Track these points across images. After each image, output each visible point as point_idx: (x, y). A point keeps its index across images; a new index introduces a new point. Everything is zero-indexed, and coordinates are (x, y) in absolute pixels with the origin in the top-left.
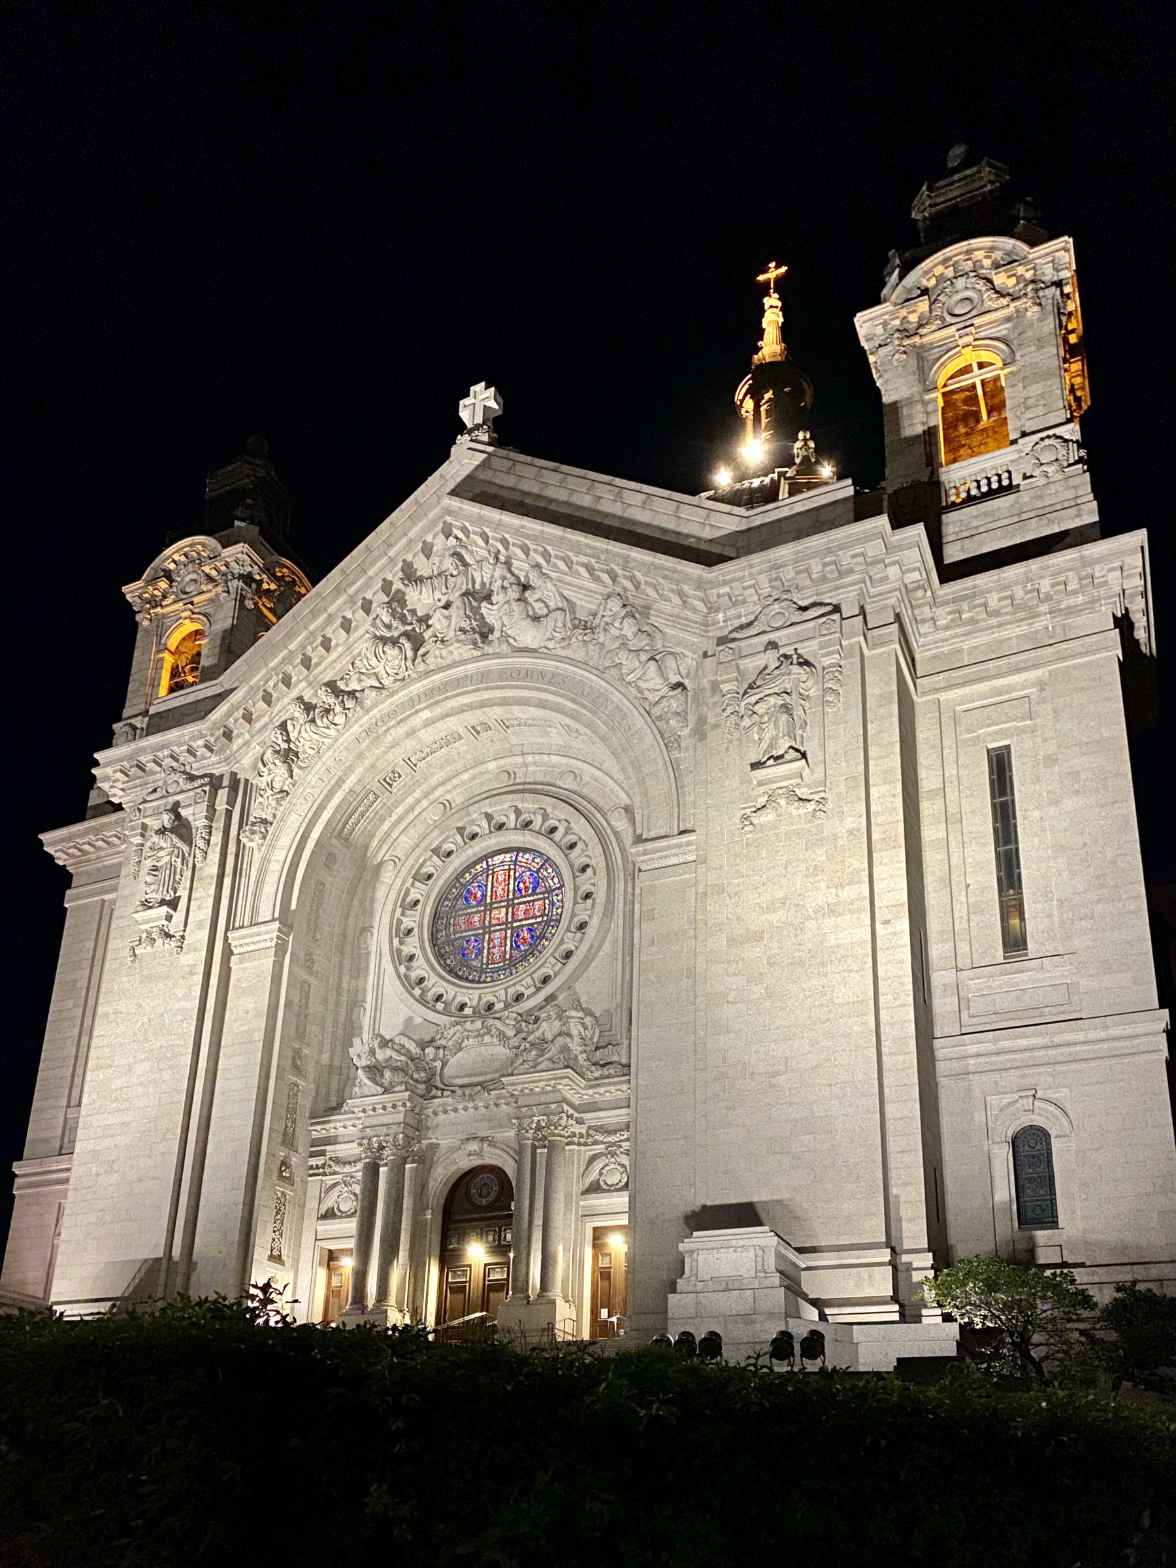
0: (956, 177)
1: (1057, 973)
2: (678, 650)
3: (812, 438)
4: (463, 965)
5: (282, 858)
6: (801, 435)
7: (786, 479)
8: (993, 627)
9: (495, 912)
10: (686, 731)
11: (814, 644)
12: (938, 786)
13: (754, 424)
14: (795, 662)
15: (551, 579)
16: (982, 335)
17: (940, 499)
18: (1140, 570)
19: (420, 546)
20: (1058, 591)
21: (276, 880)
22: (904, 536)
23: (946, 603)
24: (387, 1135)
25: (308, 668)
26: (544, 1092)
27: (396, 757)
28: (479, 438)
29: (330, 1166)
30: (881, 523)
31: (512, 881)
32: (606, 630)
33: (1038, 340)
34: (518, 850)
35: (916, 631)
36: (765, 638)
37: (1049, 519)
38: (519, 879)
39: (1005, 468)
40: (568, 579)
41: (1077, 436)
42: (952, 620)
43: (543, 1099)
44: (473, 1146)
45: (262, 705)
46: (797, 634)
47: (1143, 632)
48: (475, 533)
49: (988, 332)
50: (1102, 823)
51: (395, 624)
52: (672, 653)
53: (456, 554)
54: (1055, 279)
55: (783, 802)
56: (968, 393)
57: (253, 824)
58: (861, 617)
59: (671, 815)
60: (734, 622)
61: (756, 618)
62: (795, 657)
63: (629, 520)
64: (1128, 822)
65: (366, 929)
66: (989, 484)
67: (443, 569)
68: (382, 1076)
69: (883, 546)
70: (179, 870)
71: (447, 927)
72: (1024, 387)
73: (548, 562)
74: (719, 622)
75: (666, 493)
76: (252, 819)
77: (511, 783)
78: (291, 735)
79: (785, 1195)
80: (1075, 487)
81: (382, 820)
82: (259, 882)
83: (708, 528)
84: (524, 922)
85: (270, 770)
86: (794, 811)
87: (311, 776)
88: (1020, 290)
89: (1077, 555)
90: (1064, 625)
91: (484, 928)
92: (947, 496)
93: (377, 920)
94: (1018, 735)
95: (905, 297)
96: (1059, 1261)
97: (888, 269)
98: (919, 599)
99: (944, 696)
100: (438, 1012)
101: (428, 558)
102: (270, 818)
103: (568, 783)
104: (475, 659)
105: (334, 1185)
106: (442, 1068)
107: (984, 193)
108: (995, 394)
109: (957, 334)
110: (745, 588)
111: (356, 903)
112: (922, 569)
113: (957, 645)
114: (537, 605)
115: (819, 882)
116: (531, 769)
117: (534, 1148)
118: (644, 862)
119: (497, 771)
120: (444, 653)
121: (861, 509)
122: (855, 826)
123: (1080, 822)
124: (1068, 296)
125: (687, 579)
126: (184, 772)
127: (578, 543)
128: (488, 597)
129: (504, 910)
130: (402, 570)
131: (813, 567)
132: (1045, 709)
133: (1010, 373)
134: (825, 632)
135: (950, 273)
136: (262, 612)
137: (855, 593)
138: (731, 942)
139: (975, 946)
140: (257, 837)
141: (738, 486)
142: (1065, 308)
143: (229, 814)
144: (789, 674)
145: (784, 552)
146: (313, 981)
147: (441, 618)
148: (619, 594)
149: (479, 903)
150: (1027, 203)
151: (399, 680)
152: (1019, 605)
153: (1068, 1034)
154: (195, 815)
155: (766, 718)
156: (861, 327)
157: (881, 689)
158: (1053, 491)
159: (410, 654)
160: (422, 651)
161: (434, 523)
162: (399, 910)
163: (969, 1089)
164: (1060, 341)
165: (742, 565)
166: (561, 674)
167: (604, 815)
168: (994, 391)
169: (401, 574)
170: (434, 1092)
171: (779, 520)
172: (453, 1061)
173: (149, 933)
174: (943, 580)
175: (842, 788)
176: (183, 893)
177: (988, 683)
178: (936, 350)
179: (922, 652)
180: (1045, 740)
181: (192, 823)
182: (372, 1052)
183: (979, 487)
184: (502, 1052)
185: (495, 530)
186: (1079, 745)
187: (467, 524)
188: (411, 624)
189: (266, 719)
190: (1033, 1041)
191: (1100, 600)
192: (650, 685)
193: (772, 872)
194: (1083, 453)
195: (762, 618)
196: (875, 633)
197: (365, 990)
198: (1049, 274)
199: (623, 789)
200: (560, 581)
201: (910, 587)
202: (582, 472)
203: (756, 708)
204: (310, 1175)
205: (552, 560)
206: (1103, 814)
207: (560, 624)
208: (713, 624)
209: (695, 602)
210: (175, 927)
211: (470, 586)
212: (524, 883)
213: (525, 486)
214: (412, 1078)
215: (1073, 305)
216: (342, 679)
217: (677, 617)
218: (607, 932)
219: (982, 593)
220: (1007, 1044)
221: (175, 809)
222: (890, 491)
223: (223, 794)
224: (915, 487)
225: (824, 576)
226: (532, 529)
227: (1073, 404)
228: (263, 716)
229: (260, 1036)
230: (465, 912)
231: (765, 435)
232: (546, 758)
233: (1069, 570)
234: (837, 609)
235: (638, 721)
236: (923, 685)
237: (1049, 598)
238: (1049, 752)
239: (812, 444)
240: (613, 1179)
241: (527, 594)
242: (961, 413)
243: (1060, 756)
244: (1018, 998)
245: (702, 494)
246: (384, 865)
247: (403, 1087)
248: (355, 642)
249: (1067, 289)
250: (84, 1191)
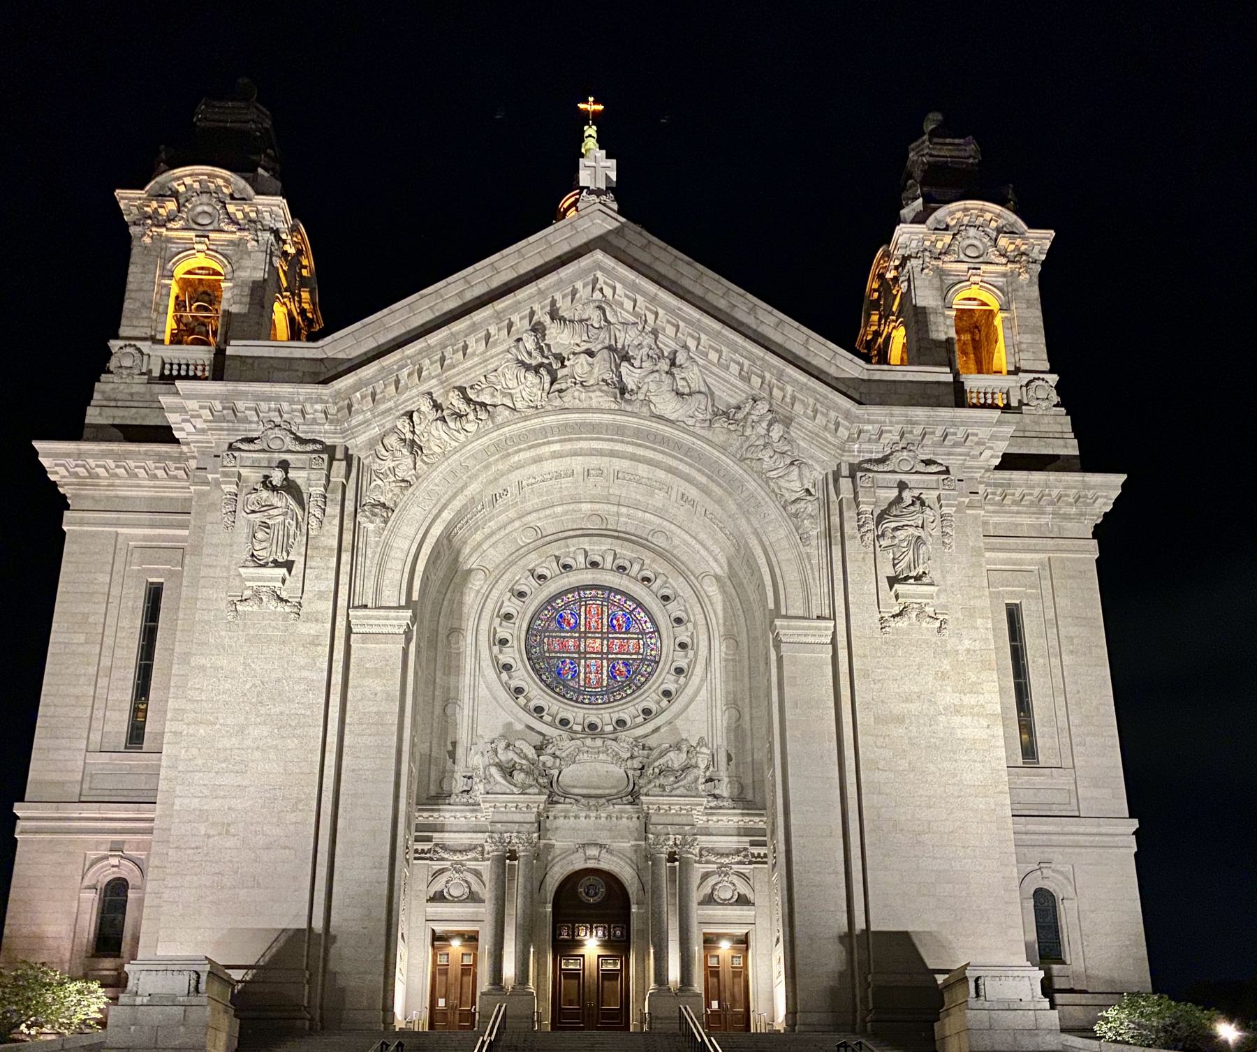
2: (810, 462)
4: (558, 683)
10: (814, 533)
15: (698, 365)
46: (924, 481)
103: (660, 541)
104: (610, 411)
116: (622, 519)
119: (589, 513)
120: (583, 396)
127: (736, 343)
129: (598, 641)
147: (585, 363)
149: (573, 629)
160: (556, 387)
166: (697, 451)
188: (547, 358)
208: (849, 451)
211: (613, 342)
212: (618, 621)
217: (817, 435)
226: (689, 315)
230: (558, 634)
232: (640, 514)
235: (773, 511)
241: (674, 370)
246: (473, 574)
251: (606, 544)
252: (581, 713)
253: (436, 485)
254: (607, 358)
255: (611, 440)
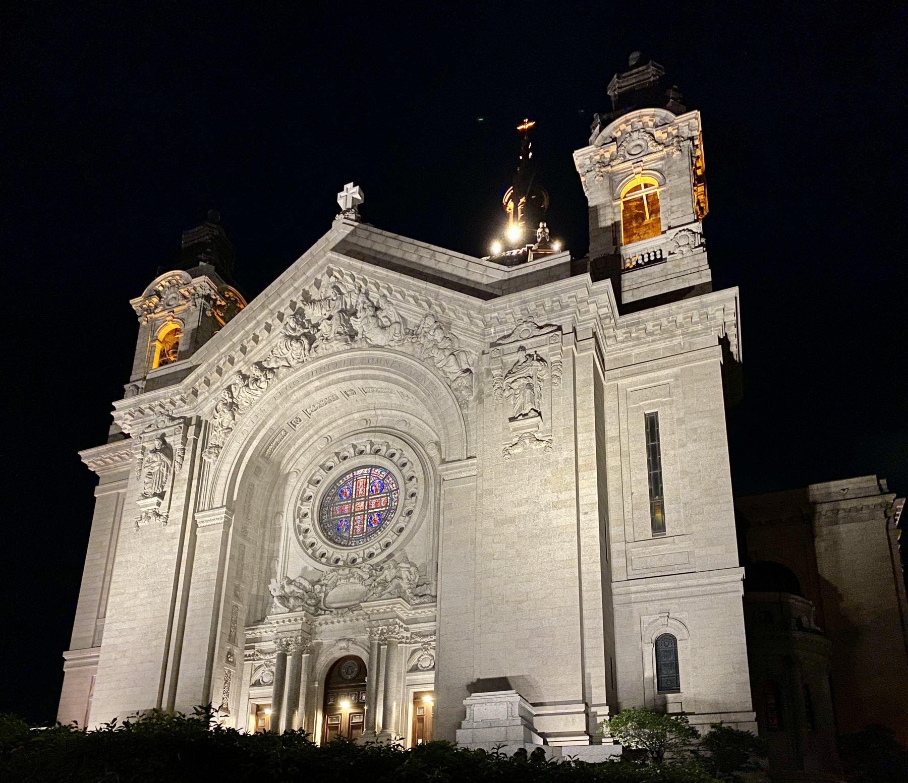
0: (634, 71)
1: (683, 545)
2: (468, 349)
3: (547, 227)
5: (228, 469)
6: (541, 225)
7: (532, 251)
8: (649, 342)
9: (357, 504)
10: (472, 398)
11: (546, 349)
12: (616, 435)
13: (514, 217)
14: (535, 359)
16: (647, 167)
17: (621, 264)
18: (734, 310)
19: (314, 281)
20: (687, 322)
21: (224, 482)
22: (599, 286)
23: (623, 327)
24: (291, 637)
25: (244, 353)
26: (385, 612)
27: (299, 407)
28: (350, 217)
29: (257, 655)
30: (586, 278)
31: (368, 485)
32: (425, 336)
33: (679, 172)
34: (372, 467)
35: (605, 343)
36: (518, 344)
37: (682, 279)
38: (372, 484)
39: (658, 248)
40: (403, 305)
41: (700, 230)
42: (626, 337)
43: (386, 616)
44: (343, 644)
45: (216, 375)
46: (537, 342)
47: (735, 348)
48: (347, 274)
49: (650, 166)
50: (709, 458)
51: (298, 328)
52: (464, 351)
53: (336, 287)
54: (690, 135)
55: (527, 441)
56: (638, 202)
57: (211, 448)
58: (573, 334)
59: (462, 448)
60: (500, 334)
61: (513, 332)
62: (535, 356)
63: (439, 271)
64: (724, 459)
65: (279, 513)
66: (649, 257)
67: (327, 295)
68: (288, 602)
69: (587, 292)
70: (165, 475)
71: (328, 512)
72: (671, 200)
73: (391, 294)
74: (491, 334)
75: (461, 255)
76: (209, 445)
77: (368, 426)
78: (234, 394)
79: (525, 673)
80: (698, 261)
81: (290, 447)
82: (214, 483)
83: (485, 277)
84: (375, 510)
85: (220, 415)
86: (534, 447)
87: (246, 419)
88: (670, 141)
89: (699, 301)
90: (690, 342)
91: (351, 513)
92: (625, 264)
93: (286, 507)
94: (663, 406)
95: (602, 142)
96: (680, 711)
97: (593, 125)
98: (607, 324)
99: (621, 382)
100: (323, 564)
101: (318, 289)
102: (221, 445)
103: (402, 427)
105: (260, 667)
106: (325, 598)
107: (650, 82)
108: (653, 201)
109: (633, 166)
110: (506, 314)
111: (273, 497)
112: (609, 306)
113: (628, 352)
114: (384, 320)
115: (548, 489)
116: (380, 418)
117: (379, 645)
118: (447, 475)
119: (359, 419)
120: (328, 346)
121: (574, 269)
122: (569, 456)
123: (697, 458)
124: (697, 146)
125: (473, 307)
126: (168, 415)
128: (354, 314)
129: (363, 503)
130: (302, 296)
131: (546, 303)
132: (678, 391)
133: (662, 191)
134: (553, 342)
135: (629, 129)
136: (218, 321)
137: (570, 319)
138: (497, 523)
139: (636, 529)
140: (213, 456)
141: (504, 254)
142: (695, 153)
143: (195, 441)
144: (531, 366)
145: (530, 293)
146: (247, 544)
147: (326, 325)
148: (433, 315)
149: (348, 499)
150: (675, 90)
151: (300, 362)
152: (664, 329)
153: (687, 581)
154: (175, 441)
155: (518, 392)
156: (577, 159)
157: (584, 376)
158: (686, 262)
159: (307, 346)
160: (314, 345)
161: (322, 267)
162: (299, 502)
163: (631, 612)
164: (692, 173)
165: (505, 300)
167: (423, 447)
168: (653, 201)
169: (301, 298)
170: (320, 612)
171: (527, 274)
172: (331, 593)
173: (147, 513)
174: (621, 314)
175: (562, 434)
176: (167, 489)
177: (646, 375)
178: (620, 176)
179: (608, 355)
180: (678, 409)
181: (173, 447)
182: (283, 587)
183: (643, 259)
184: (361, 588)
185: (359, 273)
186: (697, 412)
187: (342, 269)
188: (308, 328)
189: (218, 384)
190: (668, 585)
191: (711, 328)
192: (451, 370)
193: (521, 482)
194: (703, 240)
195: (516, 332)
196: (582, 343)
197: (278, 550)
198: (686, 133)
199: (434, 431)
200: (398, 306)
201: (602, 317)
202: (411, 240)
203: (512, 385)
204: (245, 661)
205: (393, 292)
206: (710, 453)
207: (397, 332)
208: (488, 335)
209: (478, 321)
210: (162, 510)
211: (344, 307)
212: (376, 487)
213: (377, 247)
214: (306, 603)
215: (700, 152)
216: (265, 361)
217: (467, 330)
218: (424, 517)
219: (644, 322)
220: (653, 586)
221: (162, 438)
222: (591, 260)
223: (192, 429)
224: (606, 258)
225: (553, 308)
226: (381, 274)
227: (699, 212)
228: (217, 382)
229: (214, 576)
230: (339, 503)
231: (521, 224)
232: (389, 412)
233: (694, 309)
234: (560, 328)
235: (444, 391)
236: (608, 375)
237: (682, 326)
238: (680, 416)
239: (547, 230)
240: (426, 664)
241: (378, 313)
242: (634, 214)
243: (686, 419)
244: (660, 559)
245: (483, 258)
247: (301, 609)
248: (273, 338)
249: (697, 142)
250: (107, 669)
251: (365, 438)
252: (345, 553)
253: (247, 426)
254: (338, 318)
255: (347, 370)
